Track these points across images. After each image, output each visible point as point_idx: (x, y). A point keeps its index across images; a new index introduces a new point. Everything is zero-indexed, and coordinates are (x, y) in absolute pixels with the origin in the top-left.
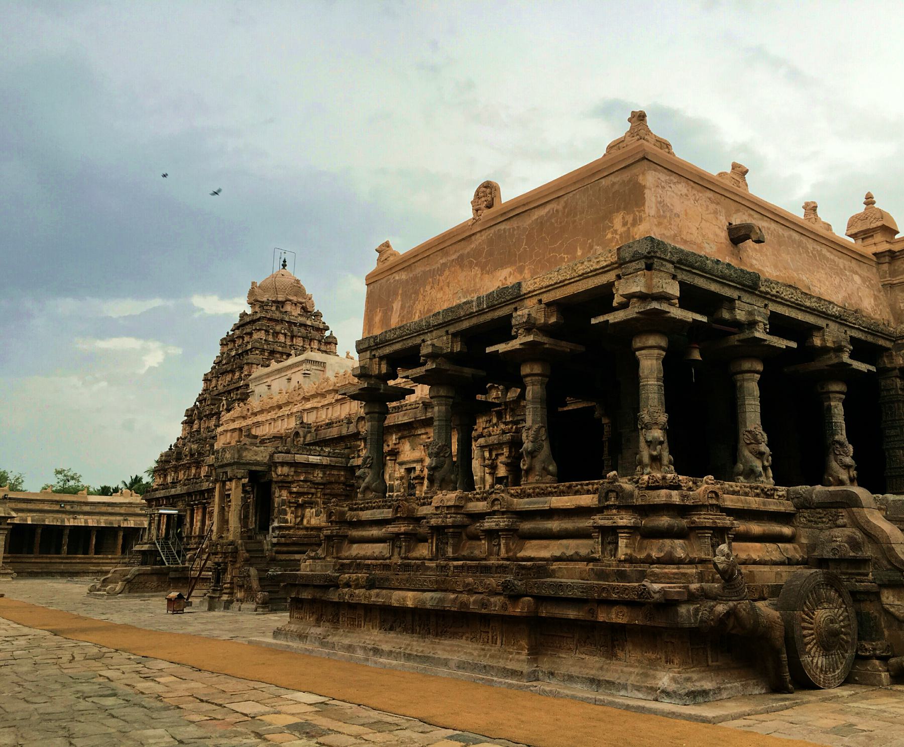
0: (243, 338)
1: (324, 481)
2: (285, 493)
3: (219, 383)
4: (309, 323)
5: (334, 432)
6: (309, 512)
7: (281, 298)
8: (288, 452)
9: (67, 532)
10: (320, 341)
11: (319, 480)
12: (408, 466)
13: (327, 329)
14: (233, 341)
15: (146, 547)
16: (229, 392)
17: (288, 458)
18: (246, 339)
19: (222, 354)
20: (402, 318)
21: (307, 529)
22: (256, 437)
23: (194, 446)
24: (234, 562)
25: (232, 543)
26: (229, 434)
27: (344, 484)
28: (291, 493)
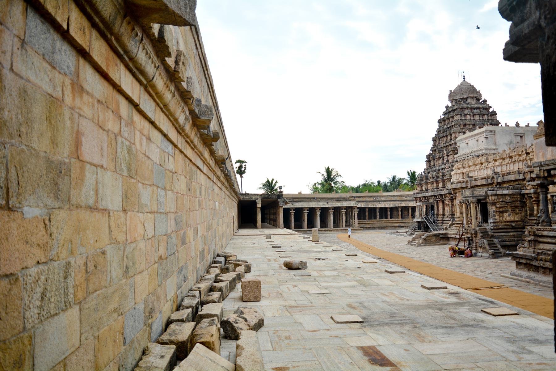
0: (449, 119)
1: (511, 201)
2: (494, 208)
3: (441, 142)
4: (481, 106)
5: (512, 177)
6: (505, 215)
7: (465, 96)
8: (493, 190)
9: (378, 210)
10: (488, 115)
11: (508, 201)
12: (552, 194)
13: (491, 107)
14: (444, 121)
15: (419, 220)
16: (446, 147)
17: (494, 192)
18: (451, 120)
19: (440, 127)
20: (553, 156)
21: (505, 222)
22: (472, 177)
23: (434, 173)
24: (476, 237)
25: (474, 229)
26: (458, 175)
27: (520, 201)
28: (496, 207)
